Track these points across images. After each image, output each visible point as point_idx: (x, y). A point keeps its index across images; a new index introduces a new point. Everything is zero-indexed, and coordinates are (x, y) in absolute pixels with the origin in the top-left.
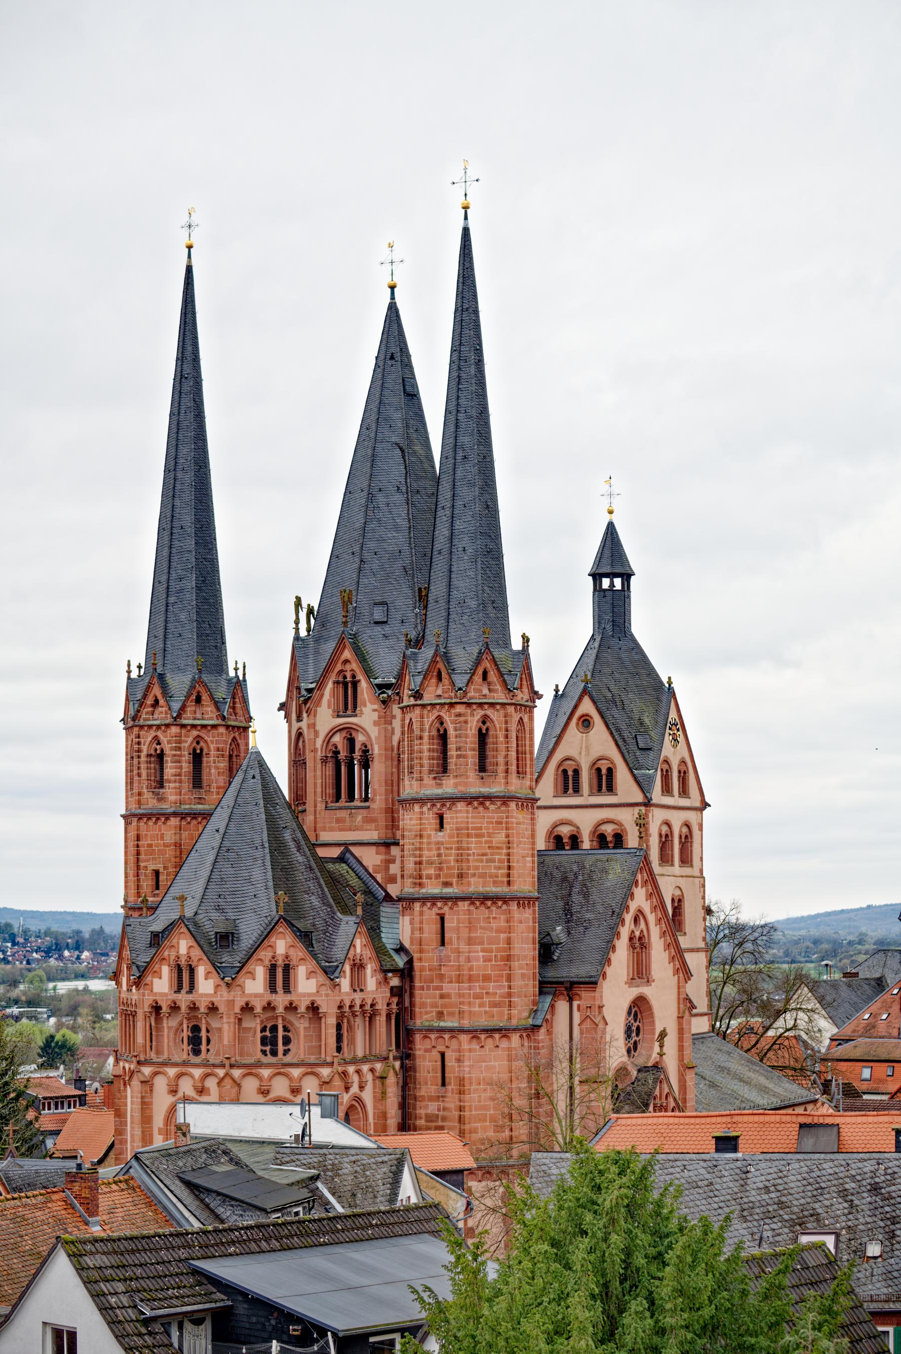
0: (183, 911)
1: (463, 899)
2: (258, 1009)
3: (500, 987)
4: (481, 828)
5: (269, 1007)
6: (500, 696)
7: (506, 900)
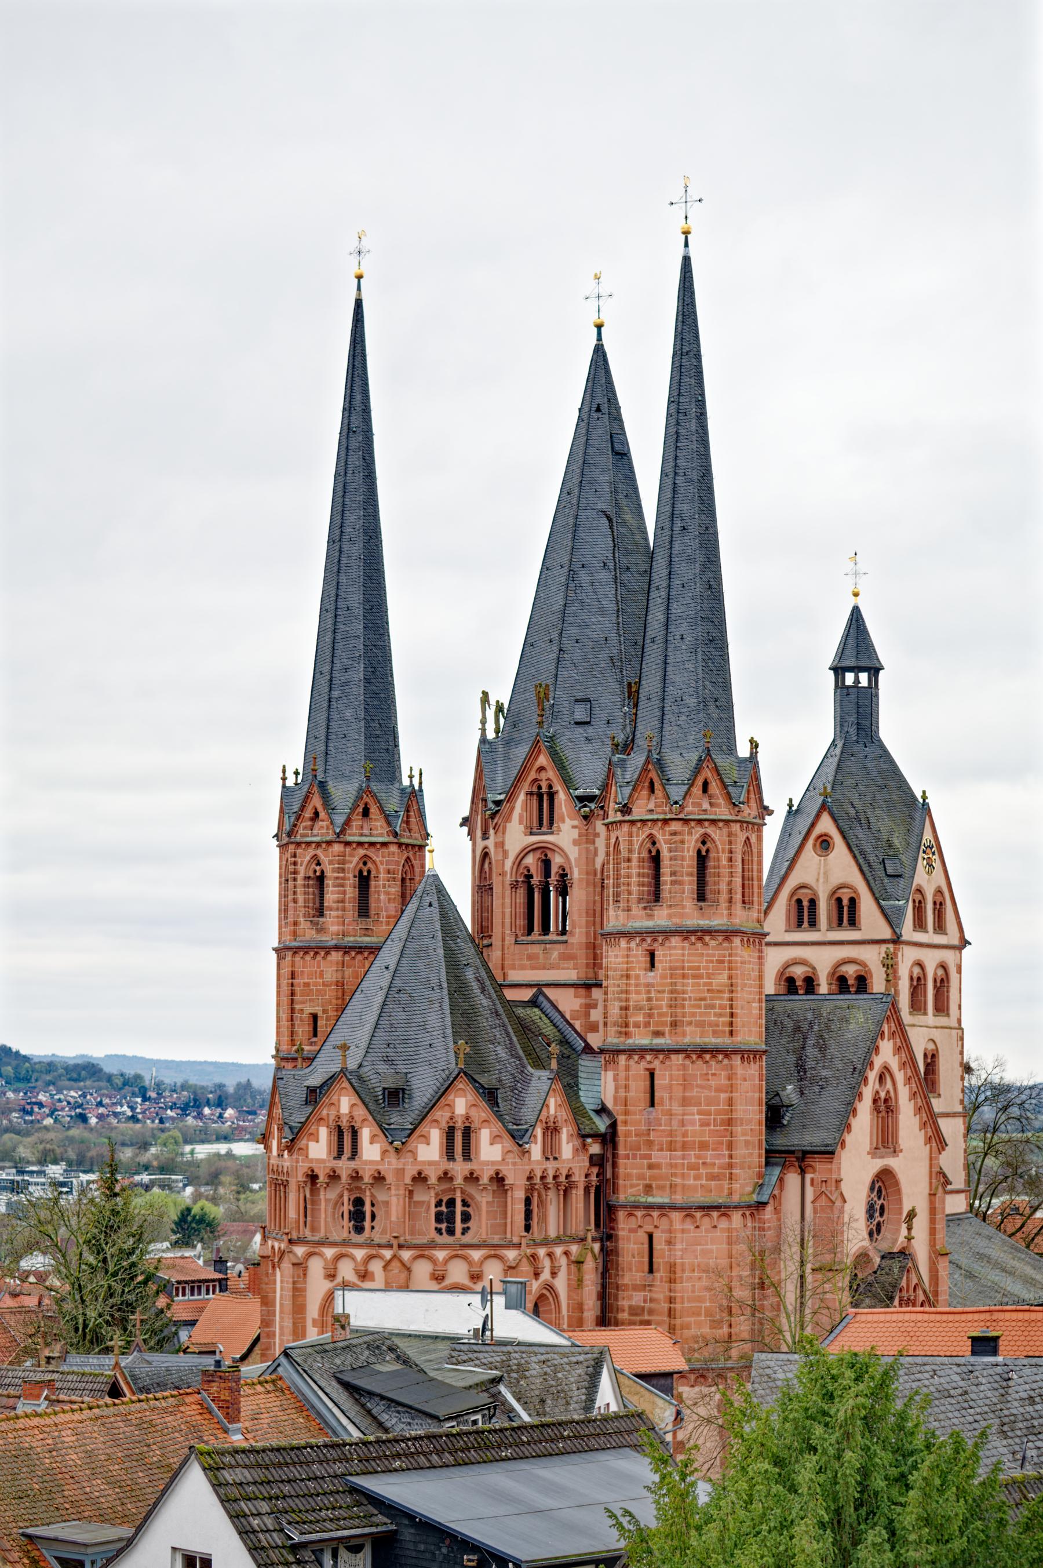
0: (345, 1062)
1: (677, 1051)
2: (433, 1180)
3: (719, 1156)
4: (698, 968)
5: (446, 1177)
6: (723, 812)
7: (727, 1053)
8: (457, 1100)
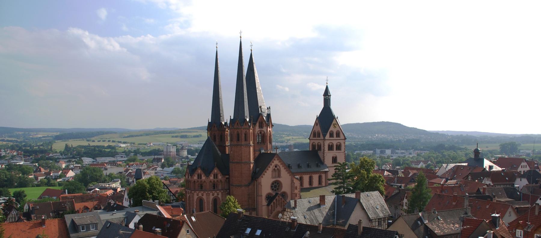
5: (214, 181)
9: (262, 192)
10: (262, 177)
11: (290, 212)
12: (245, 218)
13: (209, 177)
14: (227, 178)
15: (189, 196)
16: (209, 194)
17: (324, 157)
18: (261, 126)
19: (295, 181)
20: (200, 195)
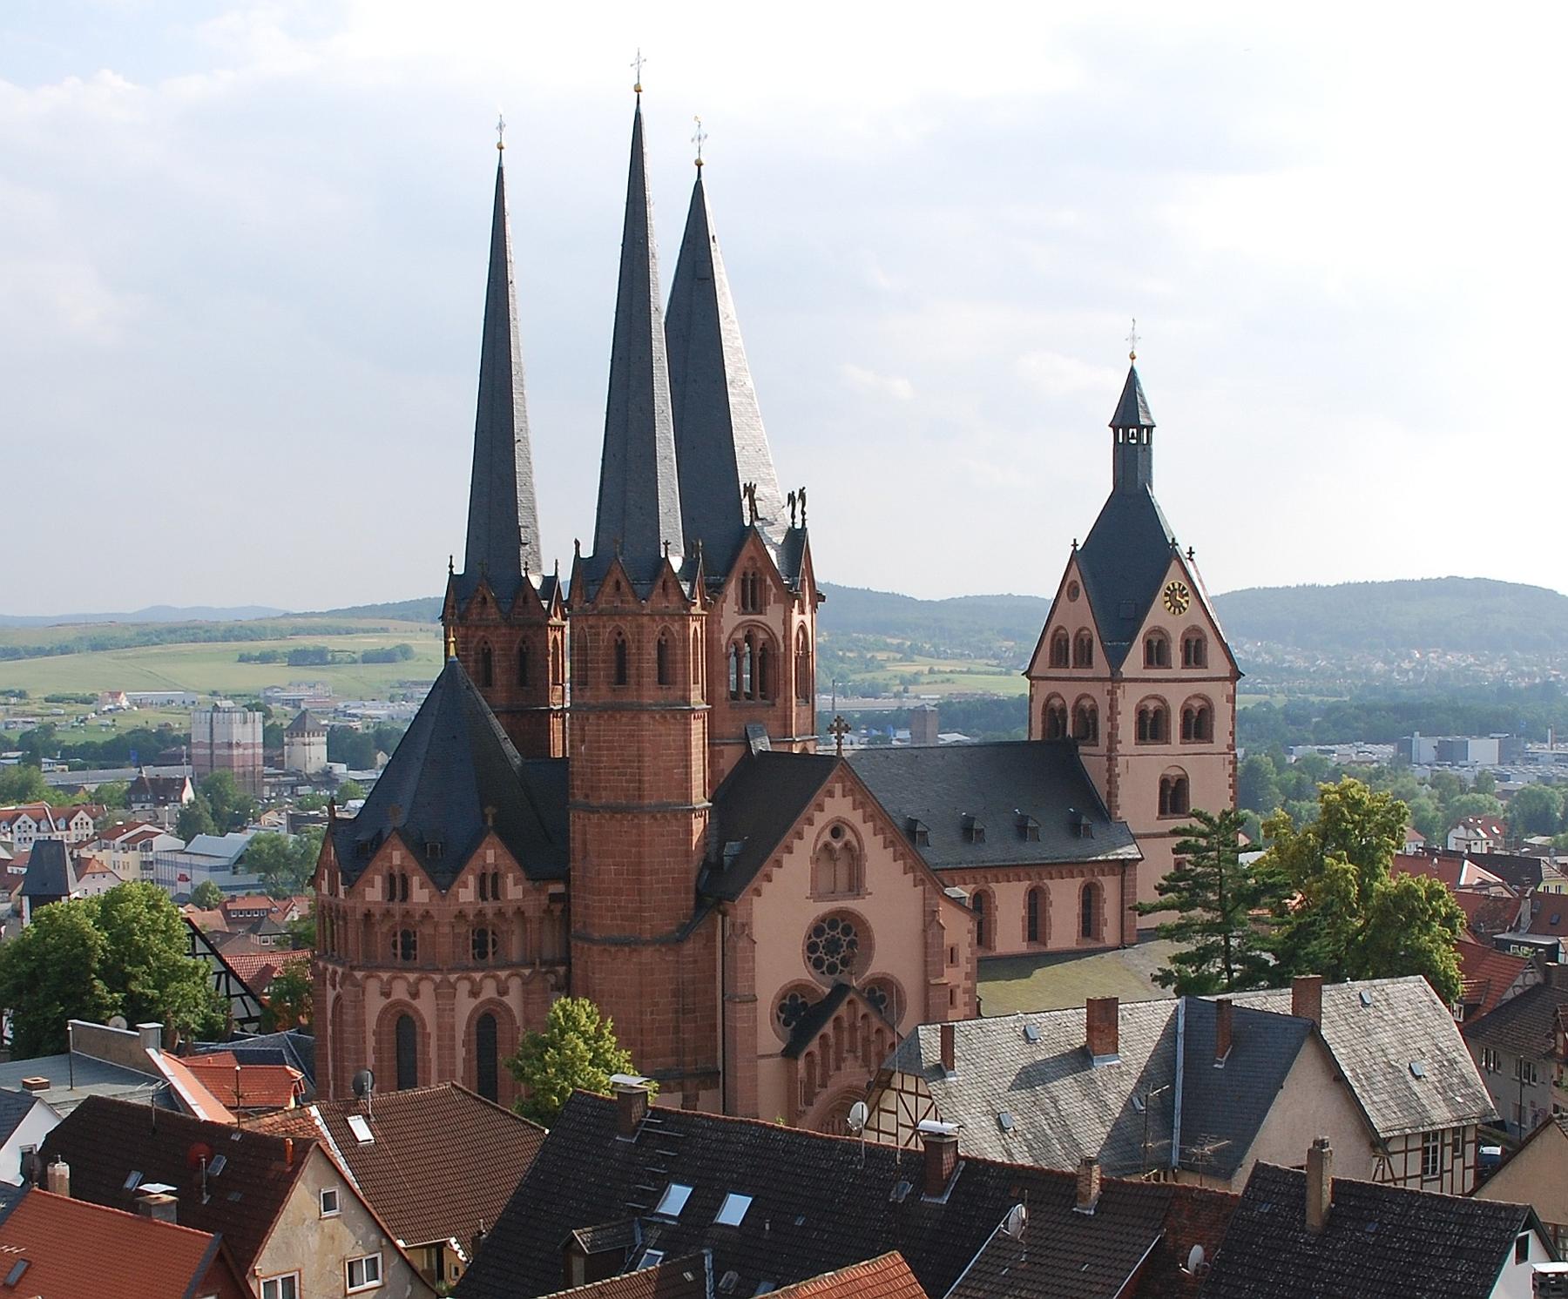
4: (612, 741)
6: (632, 606)
8: (395, 853)
9: (753, 978)
10: (758, 893)
11: (917, 1094)
12: (657, 1126)
13: (454, 888)
14: (554, 898)
15: (338, 998)
16: (453, 986)
17: (1112, 780)
18: (752, 600)
19: (946, 914)
20: (400, 992)
